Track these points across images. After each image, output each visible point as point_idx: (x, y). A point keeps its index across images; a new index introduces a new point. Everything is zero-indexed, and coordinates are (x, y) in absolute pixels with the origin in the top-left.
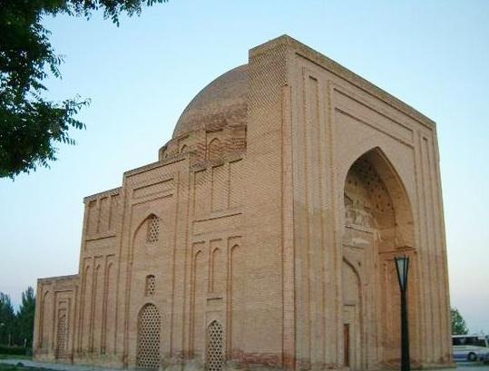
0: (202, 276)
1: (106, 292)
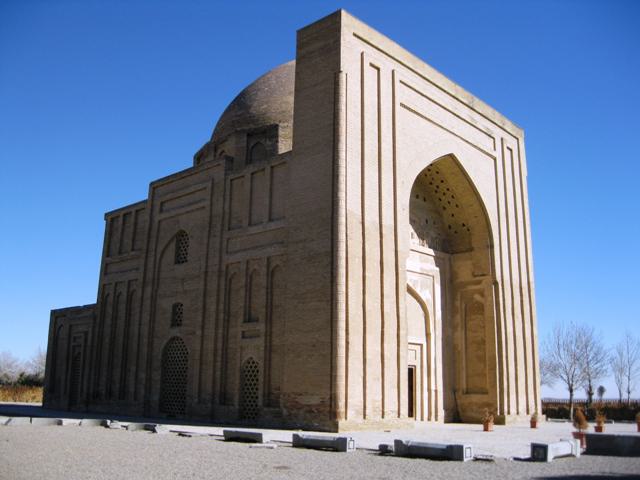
1: (128, 323)
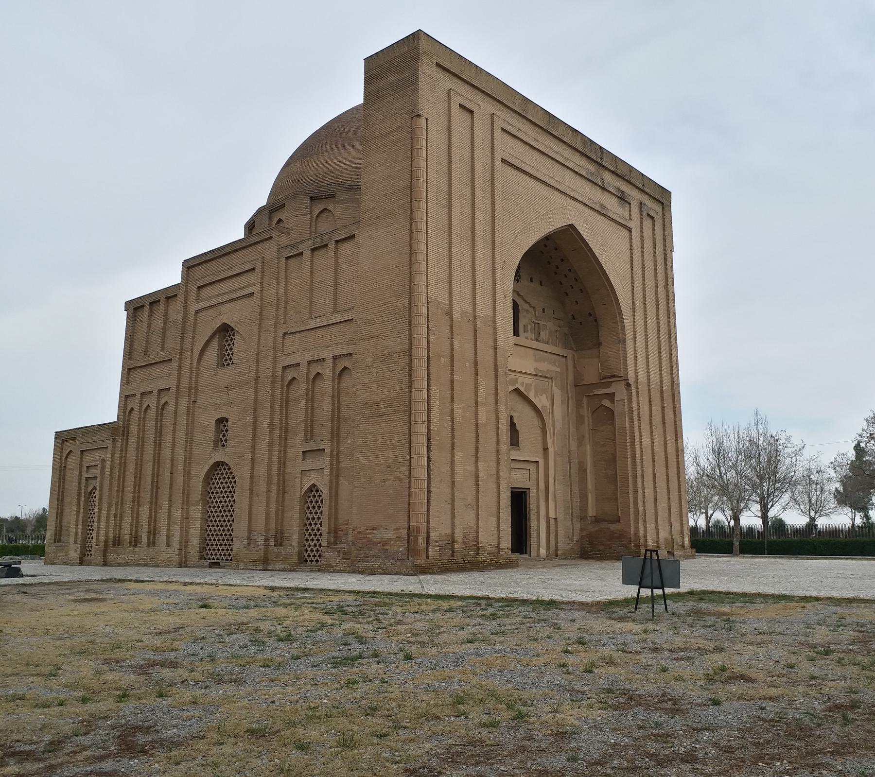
0: (298, 415)
1: (158, 446)
